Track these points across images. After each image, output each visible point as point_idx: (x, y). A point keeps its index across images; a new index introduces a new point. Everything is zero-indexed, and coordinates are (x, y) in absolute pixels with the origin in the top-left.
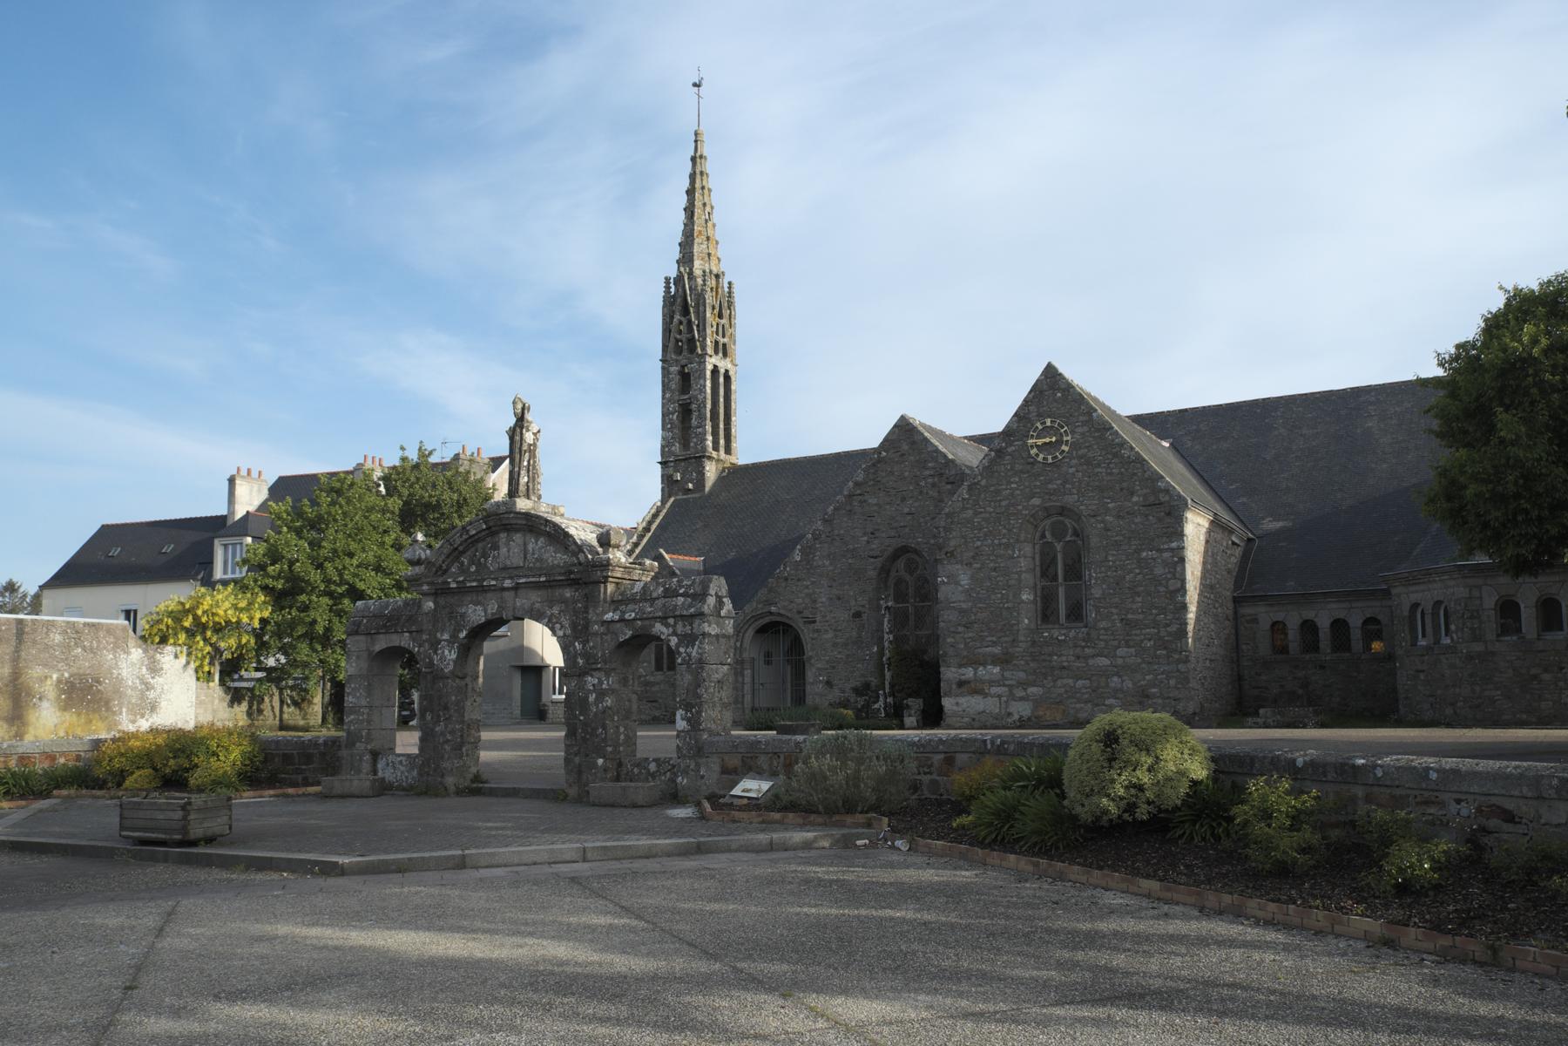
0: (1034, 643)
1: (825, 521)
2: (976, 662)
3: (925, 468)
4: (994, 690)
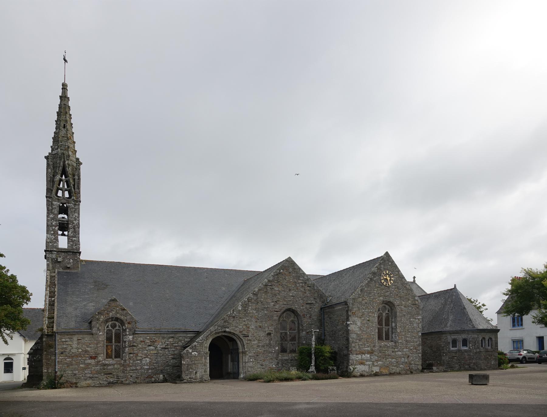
0: (380, 347)
1: (254, 294)
2: (363, 353)
3: (299, 279)
4: (367, 363)
